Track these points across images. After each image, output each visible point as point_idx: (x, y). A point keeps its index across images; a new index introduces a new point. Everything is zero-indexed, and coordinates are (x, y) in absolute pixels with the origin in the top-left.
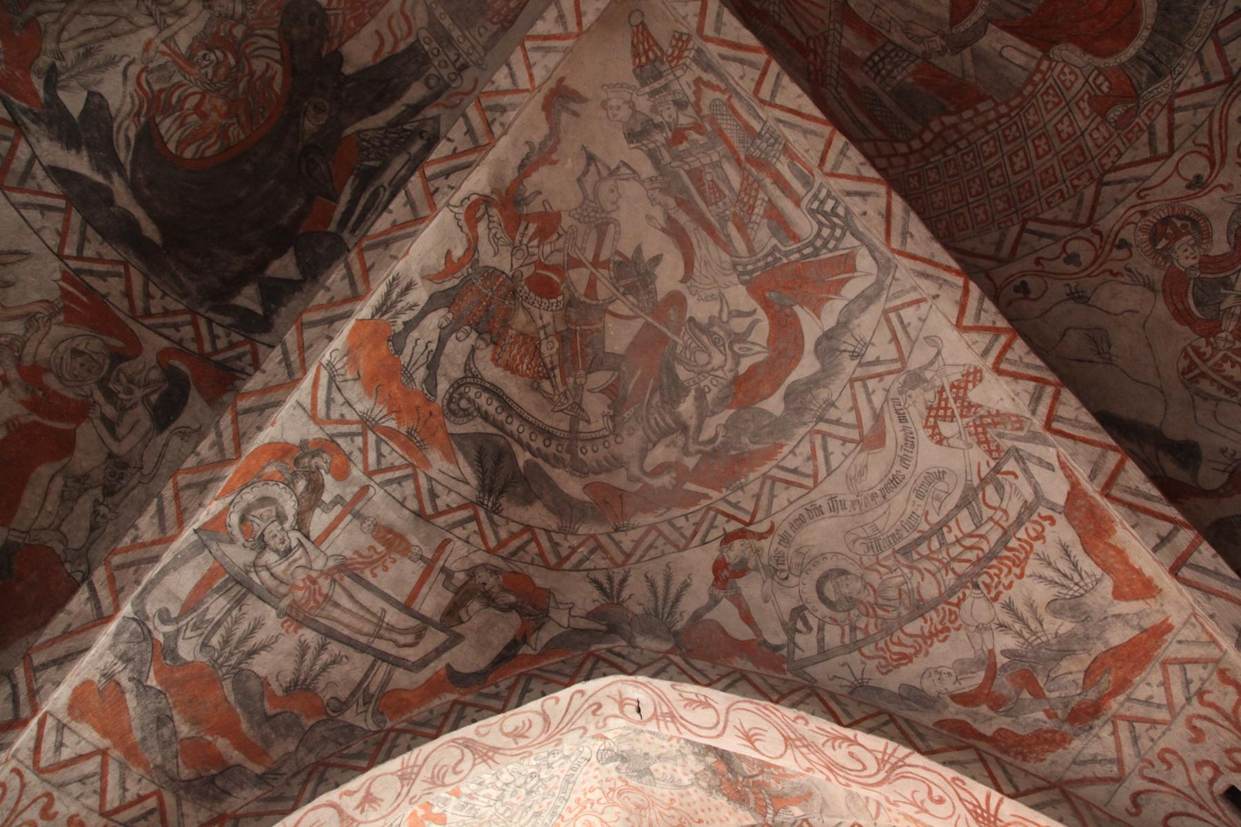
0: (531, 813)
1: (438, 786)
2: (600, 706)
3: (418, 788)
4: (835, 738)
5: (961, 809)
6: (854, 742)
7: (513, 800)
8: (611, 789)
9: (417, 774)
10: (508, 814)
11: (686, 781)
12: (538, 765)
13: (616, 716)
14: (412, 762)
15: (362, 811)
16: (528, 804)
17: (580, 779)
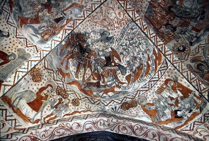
0: (133, 31)
1: (142, 127)
2: (108, 125)
3: (145, 130)
4: (63, 134)
5: (39, 137)
6: (59, 136)
7: (137, 40)
8: (112, 26)
9: (144, 133)
10: (139, 36)
11: (92, 33)
12: (129, 47)
13: (105, 121)
14: (144, 137)
15: (156, 134)
16: (133, 35)
17: (120, 33)
